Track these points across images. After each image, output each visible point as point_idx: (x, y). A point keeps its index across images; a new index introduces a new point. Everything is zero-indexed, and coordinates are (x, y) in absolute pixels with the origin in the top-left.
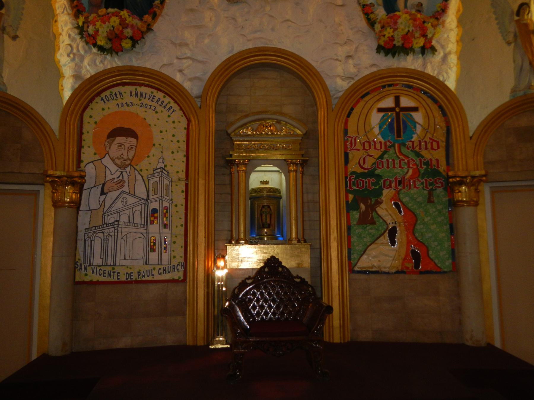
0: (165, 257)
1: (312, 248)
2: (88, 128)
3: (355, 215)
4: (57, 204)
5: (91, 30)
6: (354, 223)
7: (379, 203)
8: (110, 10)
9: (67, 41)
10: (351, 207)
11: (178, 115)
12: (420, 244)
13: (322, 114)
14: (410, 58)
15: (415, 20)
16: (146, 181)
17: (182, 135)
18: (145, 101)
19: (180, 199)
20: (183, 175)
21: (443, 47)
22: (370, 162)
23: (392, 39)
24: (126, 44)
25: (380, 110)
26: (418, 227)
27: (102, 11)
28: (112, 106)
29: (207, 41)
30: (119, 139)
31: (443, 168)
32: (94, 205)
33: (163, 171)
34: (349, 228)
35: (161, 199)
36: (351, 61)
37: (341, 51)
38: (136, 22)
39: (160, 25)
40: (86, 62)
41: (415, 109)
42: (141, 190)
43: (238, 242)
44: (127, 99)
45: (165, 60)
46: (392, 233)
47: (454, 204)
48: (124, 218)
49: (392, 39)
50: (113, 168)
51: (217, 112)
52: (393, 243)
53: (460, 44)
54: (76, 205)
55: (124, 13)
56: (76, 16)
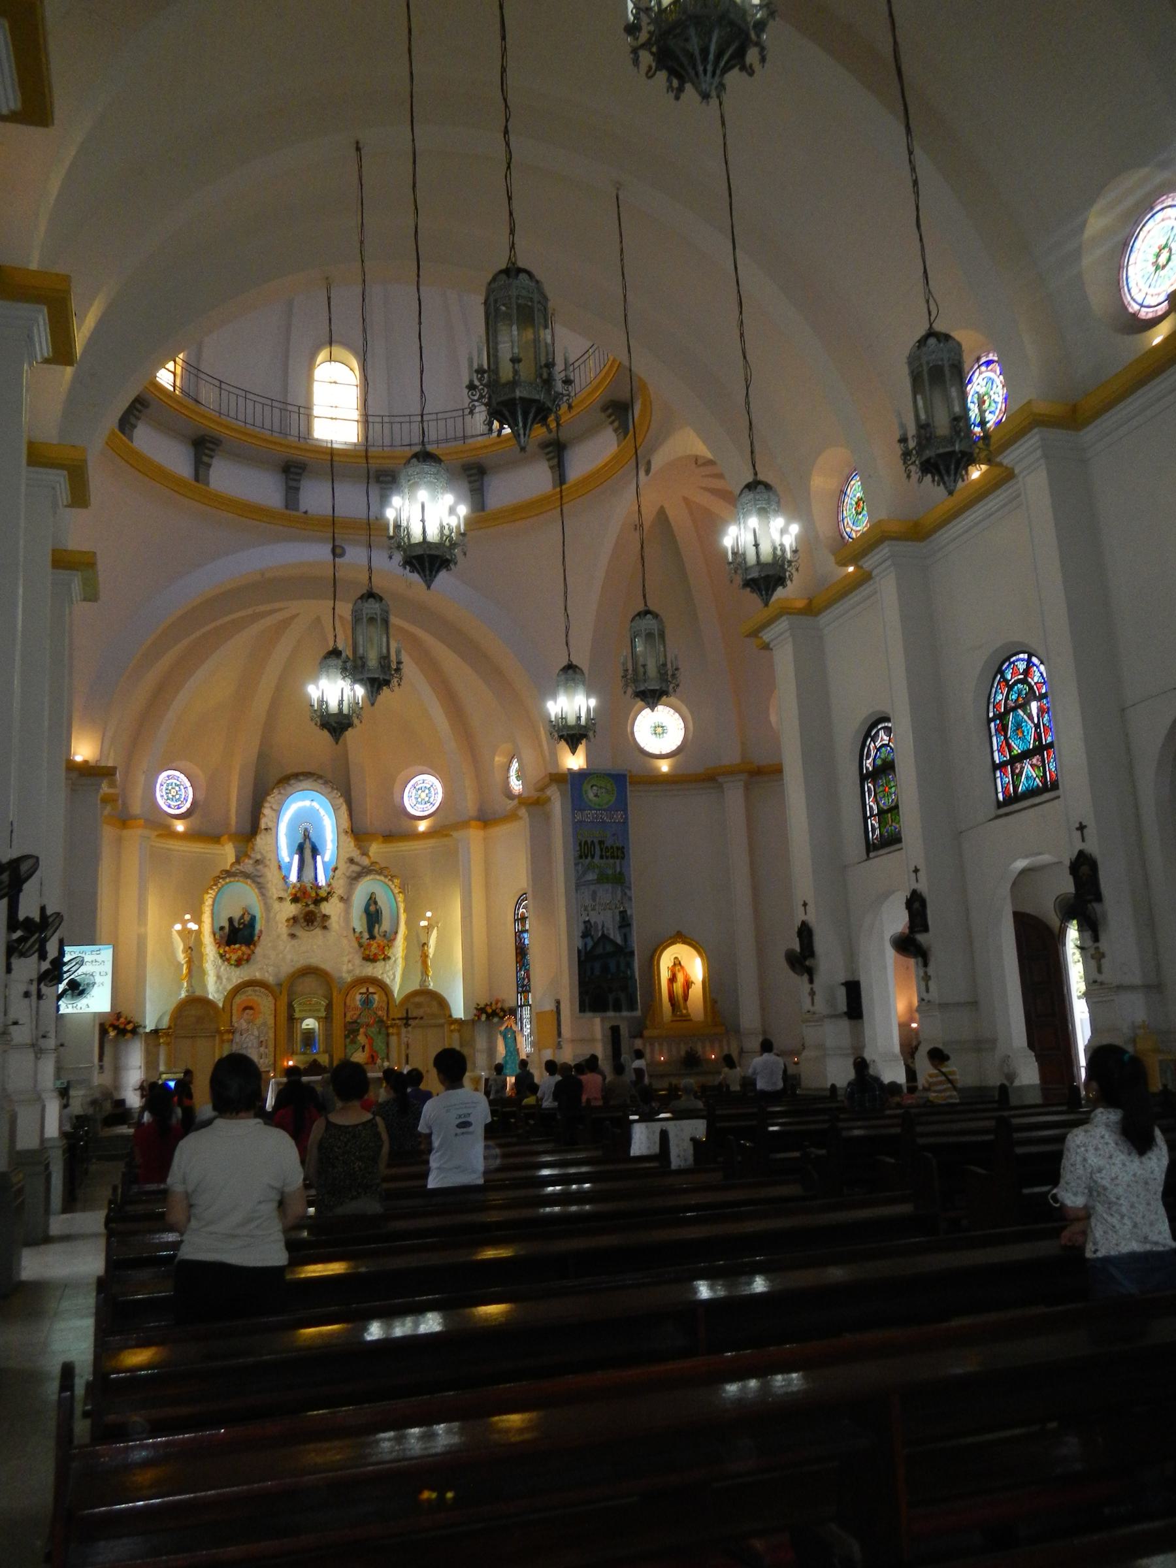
0: (267, 1061)
1: (329, 1055)
2: (235, 1007)
3: (348, 1040)
4: (222, 1041)
5: (228, 956)
6: (347, 1044)
7: (358, 1035)
8: (237, 946)
9: (212, 959)
10: (346, 1037)
11: (271, 998)
12: (375, 1052)
13: (335, 994)
14: (378, 963)
15: (379, 946)
16: (258, 1028)
17: (273, 1008)
18: (258, 993)
19: (272, 1035)
20: (273, 1025)
21: (394, 956)
22: (355, 1017)
23: (369, 955)
24: (244, 962)
25: (361, 993)
26: (374, 1044)
27: (233, 946)
28: (244, 997)
29: (281, 956)
30: (247, 1011)
31: (385, 1018)
32: (237, 1040)
33: (265, 1024)
34: (345, 1046)
35: (264, 1036)
36: (350, 965)
37: (346, 959)
38: (249, 952)
39: (258, 950)
40: (222, 969)
41: (375, 993)
42: (256, 1033)
43: (297, 1054)
44: (250, 993)
45: (260, 967)
46: (363, 1047)
47: (388, 1035)
48: (250, 1045)
49: (369, 955)
50: (245, 1024)
51: (288, 995)
52: (364, 1051)
53: (405, 951)
54: (232, 1041)
55: (244, 948)
56: (219, 947)
